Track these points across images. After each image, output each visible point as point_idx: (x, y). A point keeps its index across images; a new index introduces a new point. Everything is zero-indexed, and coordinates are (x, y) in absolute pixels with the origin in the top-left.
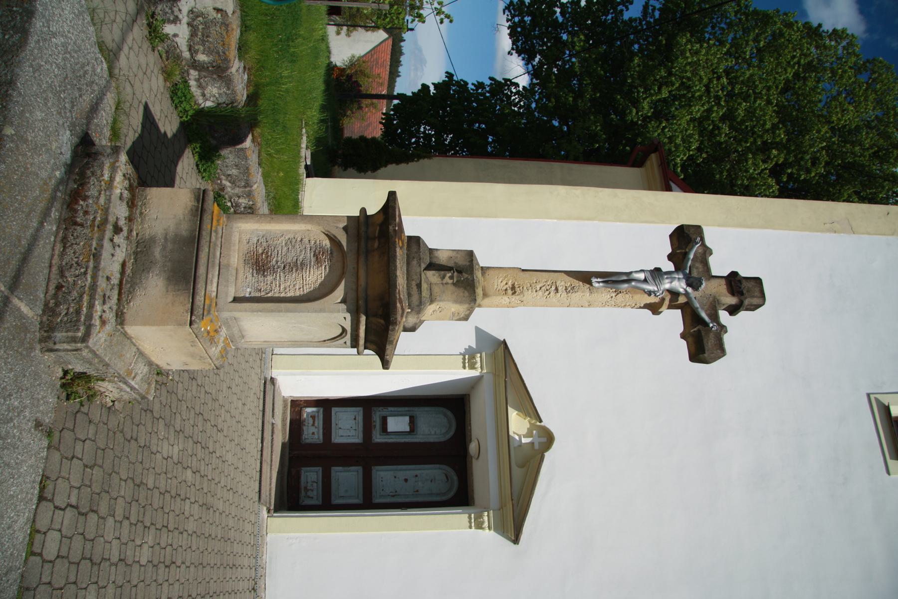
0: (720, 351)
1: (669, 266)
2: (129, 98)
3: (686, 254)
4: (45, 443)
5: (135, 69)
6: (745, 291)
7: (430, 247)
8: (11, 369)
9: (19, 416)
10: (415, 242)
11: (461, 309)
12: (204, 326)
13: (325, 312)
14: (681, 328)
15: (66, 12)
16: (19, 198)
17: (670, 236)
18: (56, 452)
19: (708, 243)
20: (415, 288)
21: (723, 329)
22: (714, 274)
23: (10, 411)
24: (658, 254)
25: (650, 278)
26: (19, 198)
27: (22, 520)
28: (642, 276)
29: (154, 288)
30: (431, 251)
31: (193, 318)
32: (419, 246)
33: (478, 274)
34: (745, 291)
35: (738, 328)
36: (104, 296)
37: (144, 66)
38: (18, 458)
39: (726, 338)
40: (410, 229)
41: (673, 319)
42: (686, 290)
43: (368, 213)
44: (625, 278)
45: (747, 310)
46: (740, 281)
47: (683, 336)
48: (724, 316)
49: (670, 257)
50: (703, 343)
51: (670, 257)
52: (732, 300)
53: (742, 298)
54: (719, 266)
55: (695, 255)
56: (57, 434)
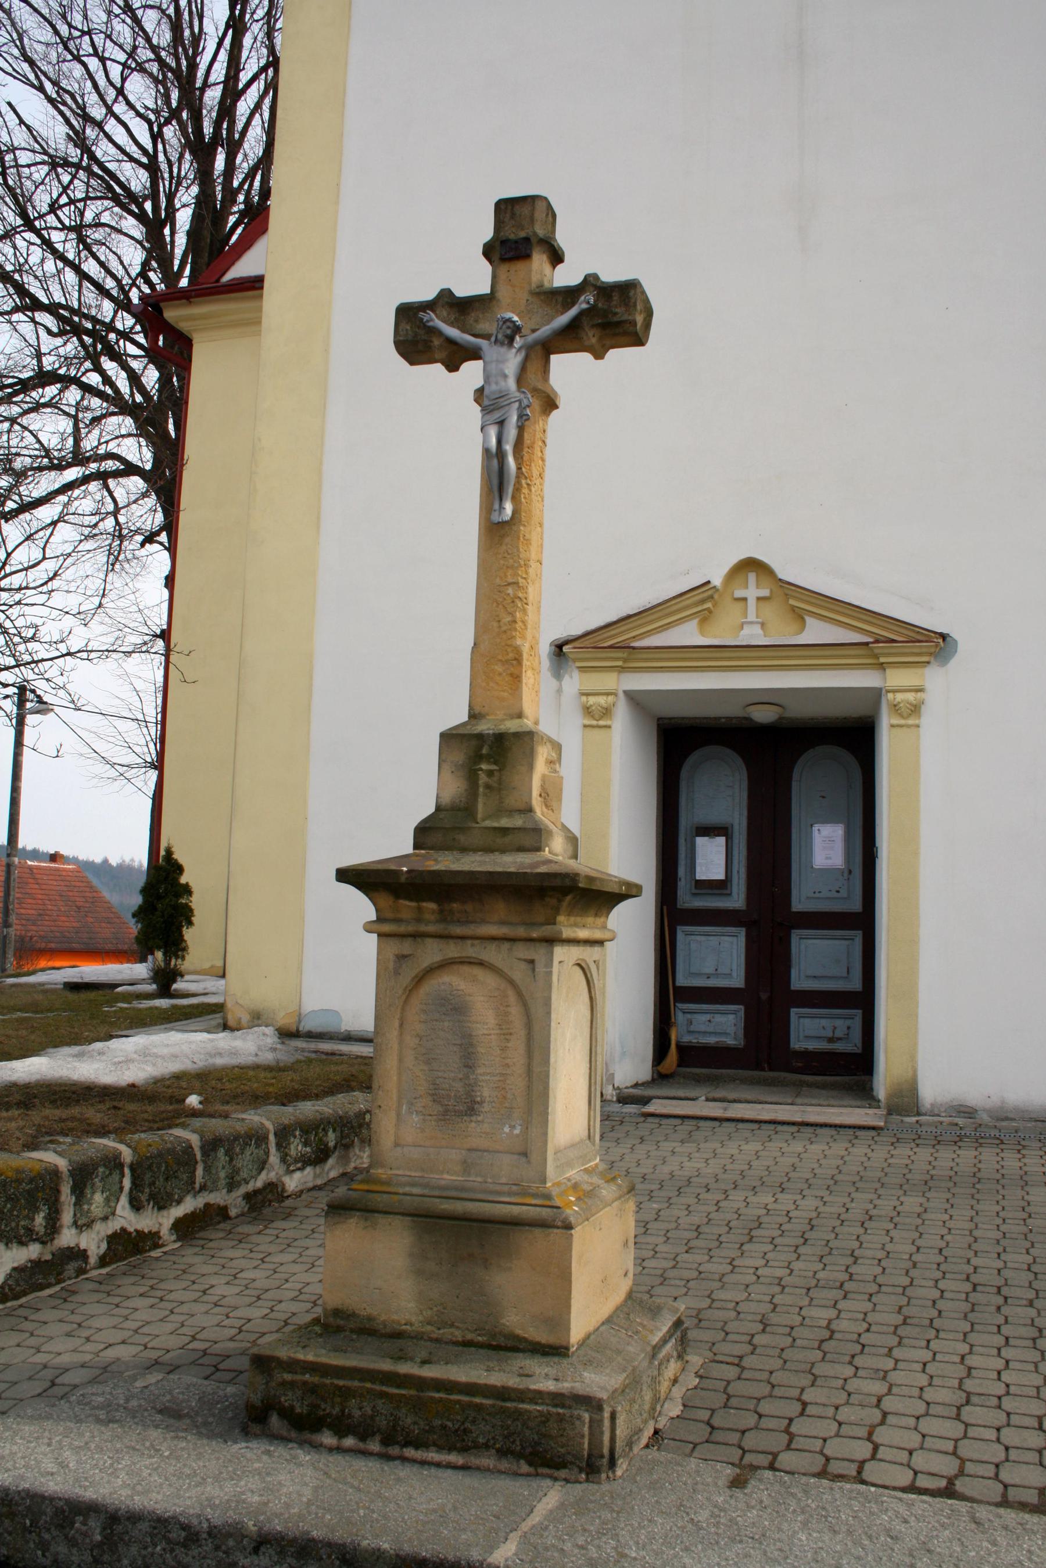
0: (627, 292)
1: (472, 372)
2: (133, 1350)
3: (450, 341)
4: (768, 1474)
5: (78, 1342)
6: (520, 232)
7: (433, 810)
8: (650, 1521)
9: (724, 1510)
10: (424, 833)
11: (542, 754)
12: (573, 1211)
13: (549, 998)
14: (586, 357)
15: (15, 1448)
16: (362, 1512)
17: (412, 363)
18: (780, 1458)
19: (429, 295)
20: (507, 840)
21: (590, 282)
22: (488, 291)
23: (718, 1523)
24: (449, 394)
25: (496, 415)
26: (362, 1512)
27: (895, 1505)
28: (493, 432)
29: (512, 1294)
30: (438, 808)
31: (560, 1224)
32: (430, 828)
33: (484, 727)
34: (520, 232)
35: (588, 252)
36: (521, 1375)
37: (68, 1328)
38: (794, 1511)
39: (608, 276)
40: (406, 847)
41: (568, 369)
42: (519, 350)
43: (373, 916)
44: (495, 462)
45: (554, 231)
46: (504, 242)
47: (599, 355)
48: (566, 276)
49: (453, 367)
50: (611, 316)
51: (453, 367)
52: (539, 260)
53: (534, 240)
54: (474, 278)
55: (451, 324)
56: (749, 1458)
